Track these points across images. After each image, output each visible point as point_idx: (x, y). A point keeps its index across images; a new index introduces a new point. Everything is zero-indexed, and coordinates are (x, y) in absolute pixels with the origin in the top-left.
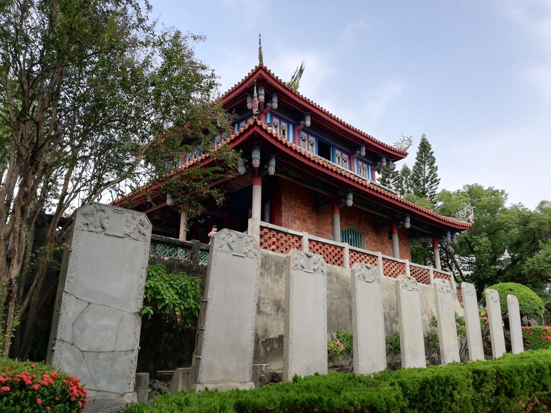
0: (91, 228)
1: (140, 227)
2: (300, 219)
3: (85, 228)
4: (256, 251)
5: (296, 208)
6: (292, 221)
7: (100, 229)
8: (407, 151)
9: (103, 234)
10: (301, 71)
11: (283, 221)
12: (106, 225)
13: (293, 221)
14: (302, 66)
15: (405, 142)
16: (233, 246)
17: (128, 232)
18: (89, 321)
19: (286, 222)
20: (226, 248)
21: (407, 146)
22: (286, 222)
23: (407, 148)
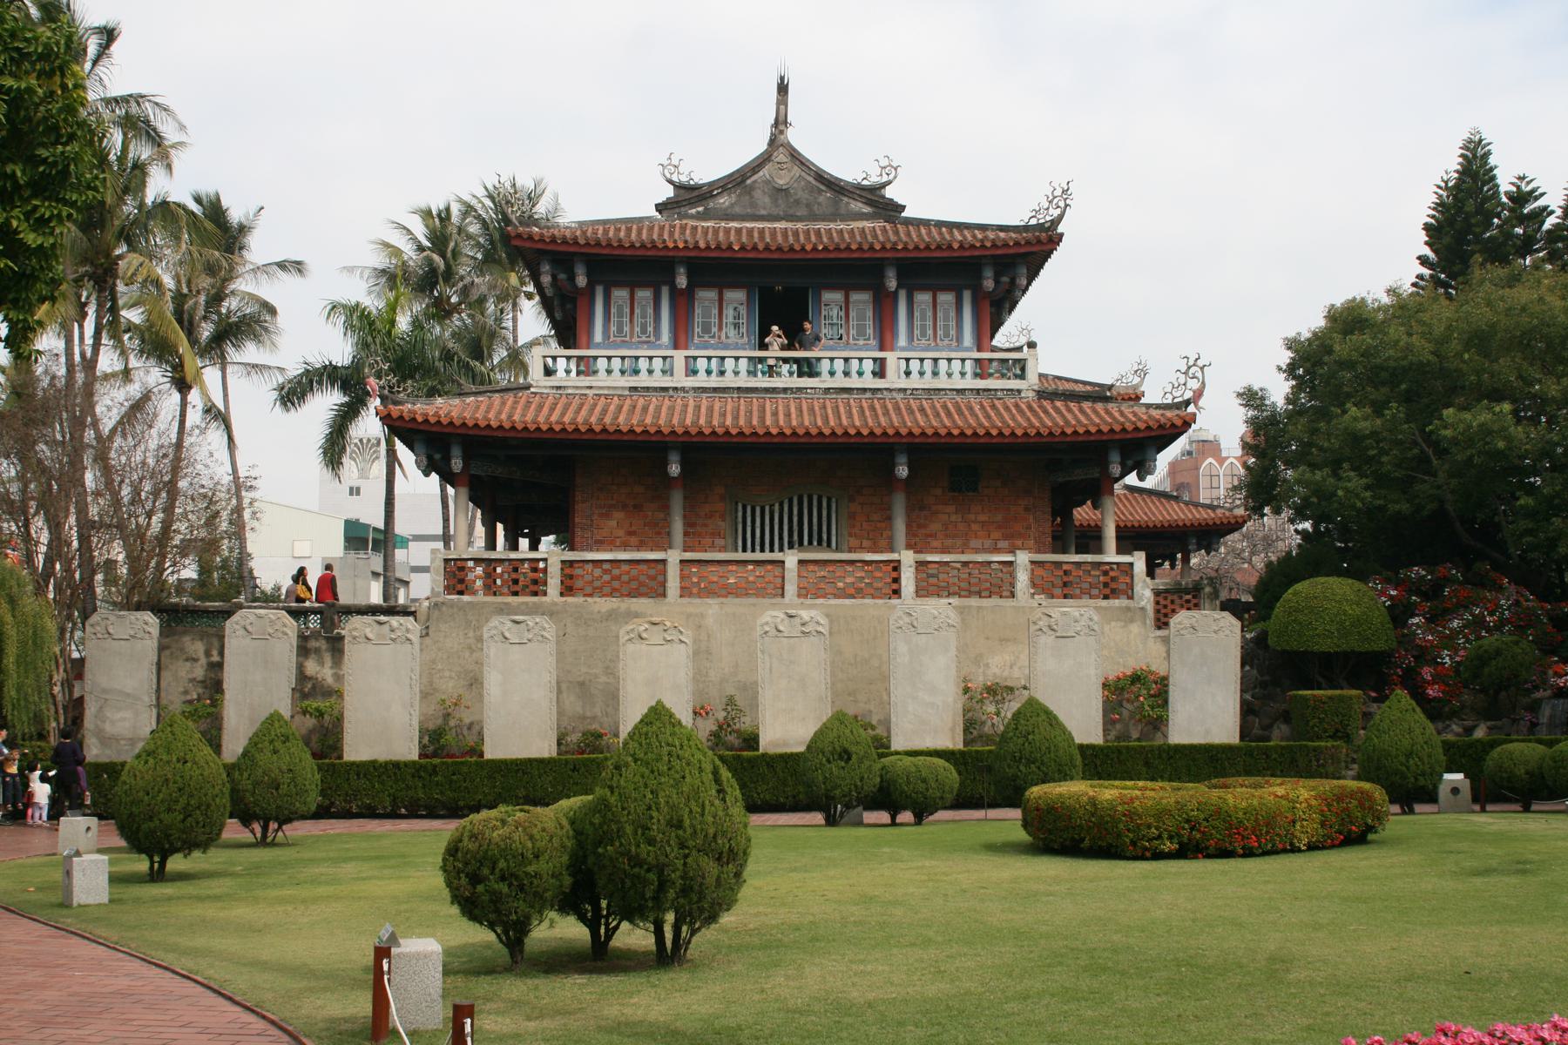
0: (99, 636)
1: (145, 627)
2: (624, 507)
3: (94, 637)
4: (285, 629)
5: (615, 487)
6: (601, 515)
7: (106, 636)
8: (1060, 229)
9: (110, 640)
10: (783, 89)
11: (577, 520)
12: (111, 631)
13: (607, 516)
14: (782, 78)
15: (1055, 201)
16: (249, 628)
17: (132, 633)
18: (108, 714)
19: (584, 521)
20: (242, 632)
21: (1058, 211)
22: (584, 521)
23: (1056, 222)
